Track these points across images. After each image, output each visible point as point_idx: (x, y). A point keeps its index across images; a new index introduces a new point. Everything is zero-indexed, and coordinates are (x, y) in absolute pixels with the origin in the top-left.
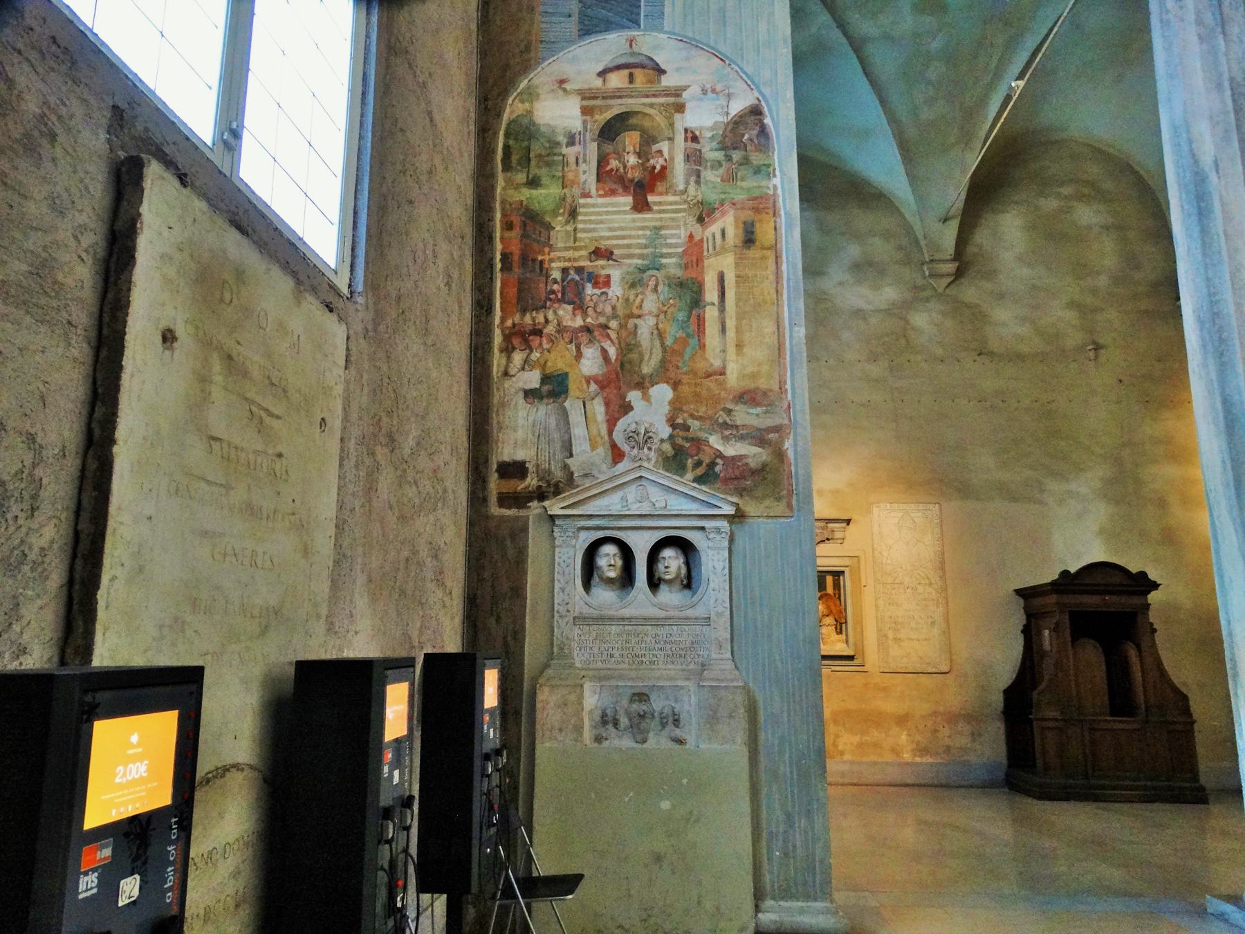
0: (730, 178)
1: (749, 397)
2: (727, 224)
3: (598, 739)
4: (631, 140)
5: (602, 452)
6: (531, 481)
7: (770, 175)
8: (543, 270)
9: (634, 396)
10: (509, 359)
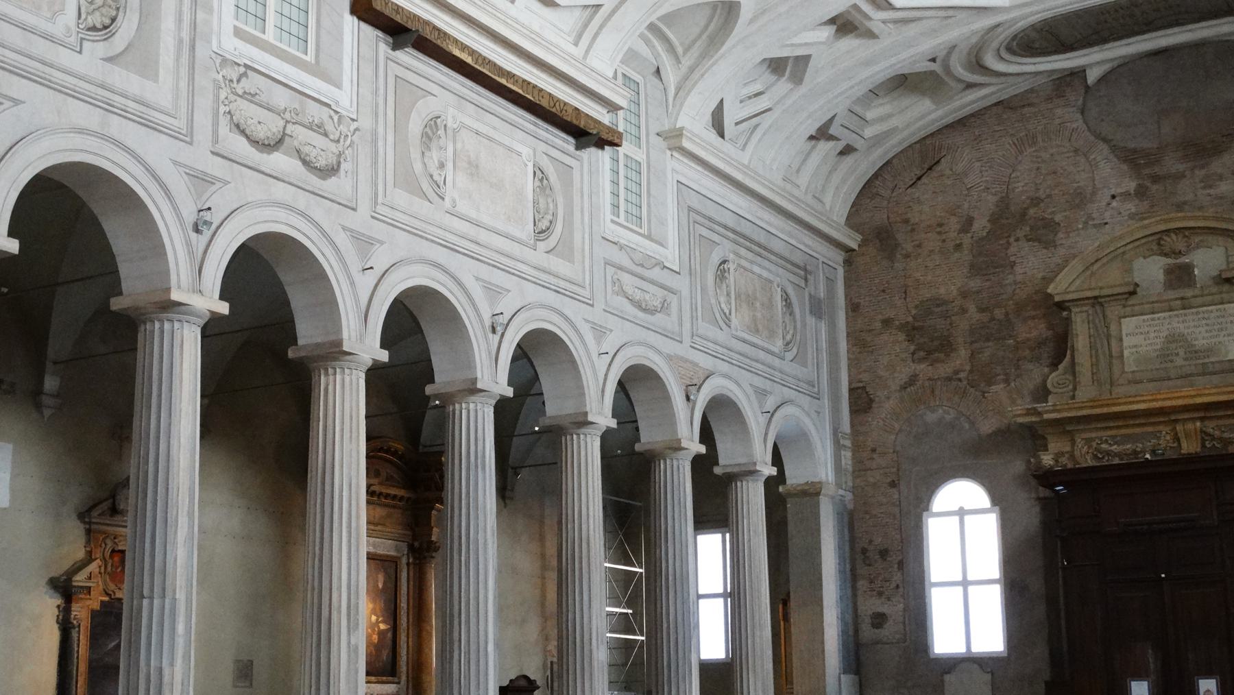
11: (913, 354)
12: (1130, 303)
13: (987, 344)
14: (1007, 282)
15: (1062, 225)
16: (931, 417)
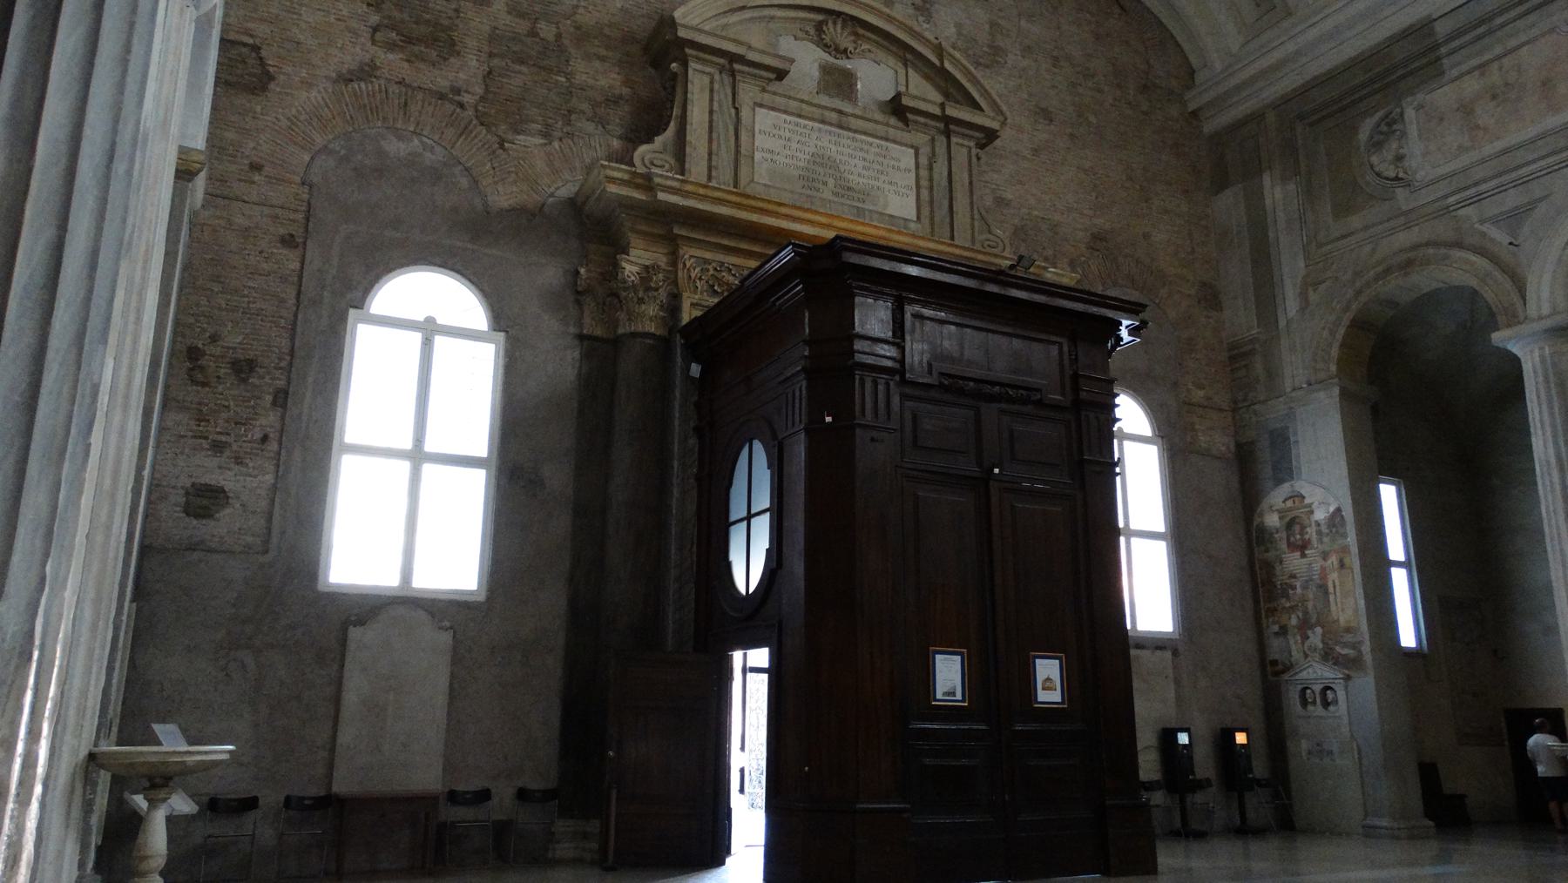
1: (1348, 630)
2: (1333, 560)
4: (1297, 528)
6: (1280, 667)
8: (1275, 586)
9: (1310, 633)
10: (1268, 621)
11: (375, 29)
12: (776, 86)
13: (517, 67)
16: (395, 147)
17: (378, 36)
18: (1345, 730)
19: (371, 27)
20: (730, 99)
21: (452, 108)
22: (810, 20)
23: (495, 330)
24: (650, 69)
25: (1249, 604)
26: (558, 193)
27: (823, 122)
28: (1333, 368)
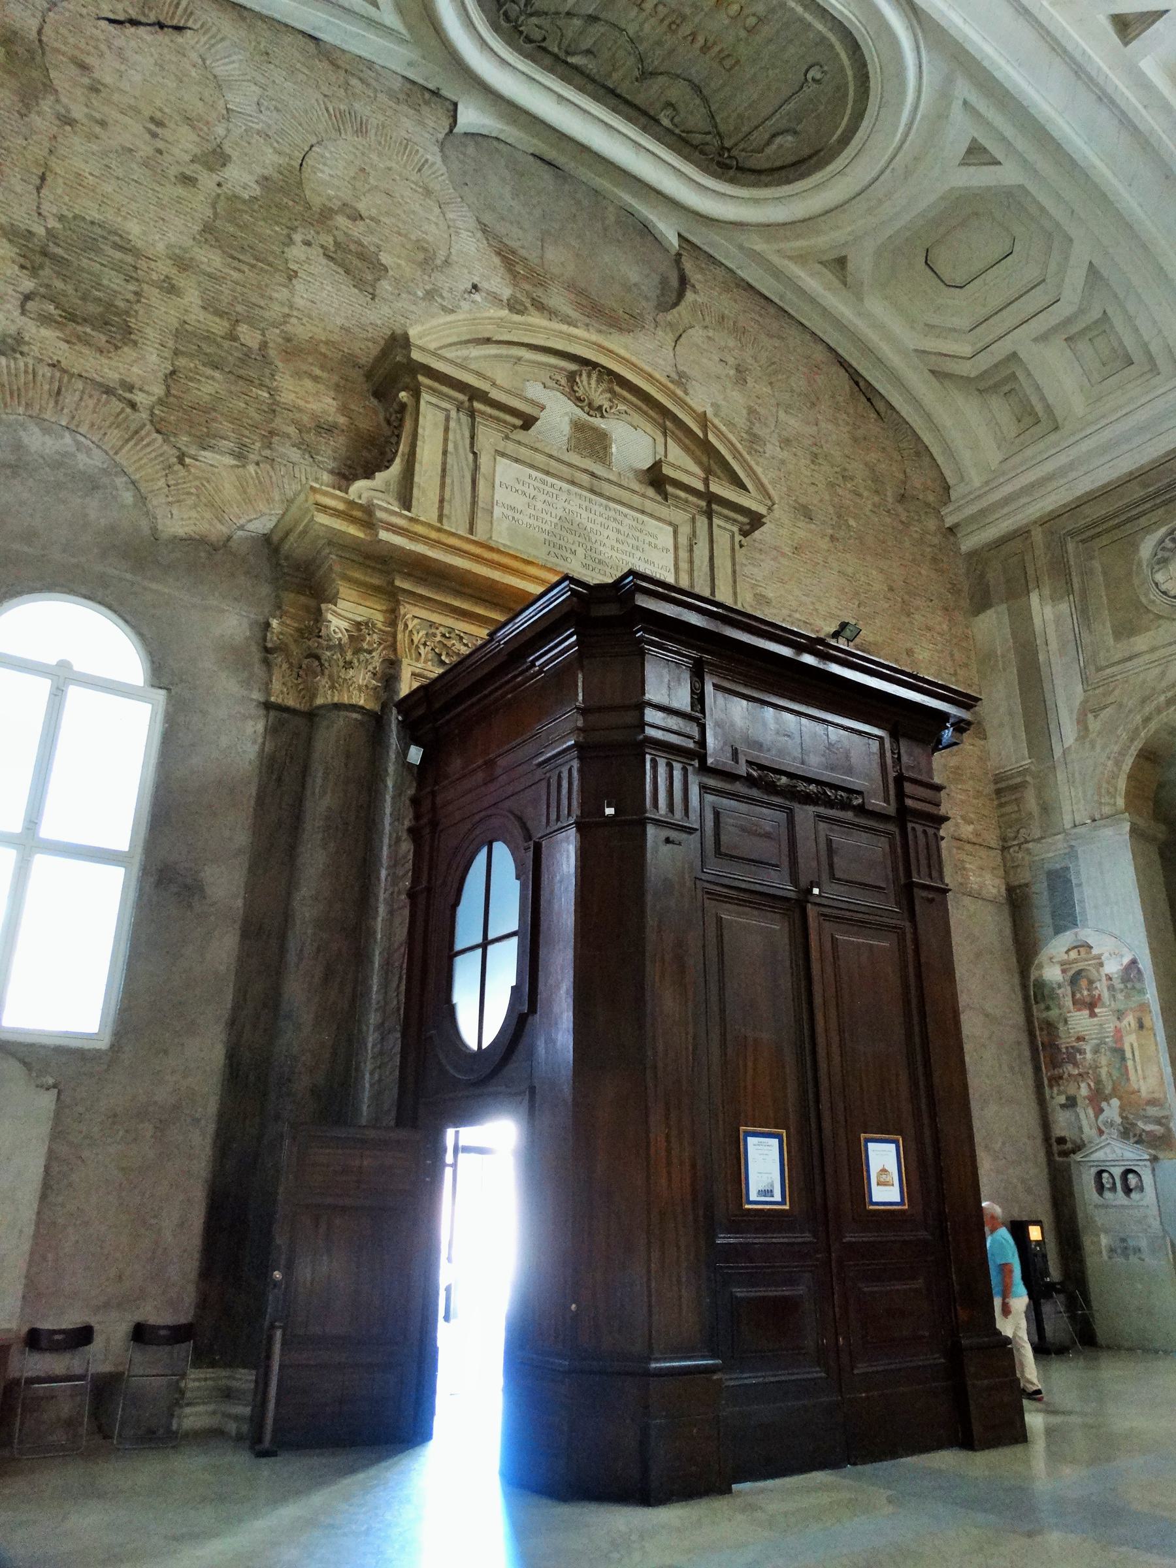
0: (1128, 997)
1: (1153, 1102)
2: (1130, 1019)
3: (1110, 1258)
4: (1083, 983)
5: (1094, 1132)
6: (1069, 1146)
7: (1145, 994)
8: (1059, 1049)
9: (1104, 1105)
11: (28, 297)
12: (520, 435)
13: (209, 371)
14: (275, 295)
15: (391, 273)
17: (30, 305)
18: (1156, 1224)
19: (22, 293)
20: (468, 441)
21: (121, 405)
22: (562, 369)
23: (152, 686)
24: (372, 399)
25: (1029, 1070)
26: (250, 527)
27: (573, 483)
28: (1121, 802)
